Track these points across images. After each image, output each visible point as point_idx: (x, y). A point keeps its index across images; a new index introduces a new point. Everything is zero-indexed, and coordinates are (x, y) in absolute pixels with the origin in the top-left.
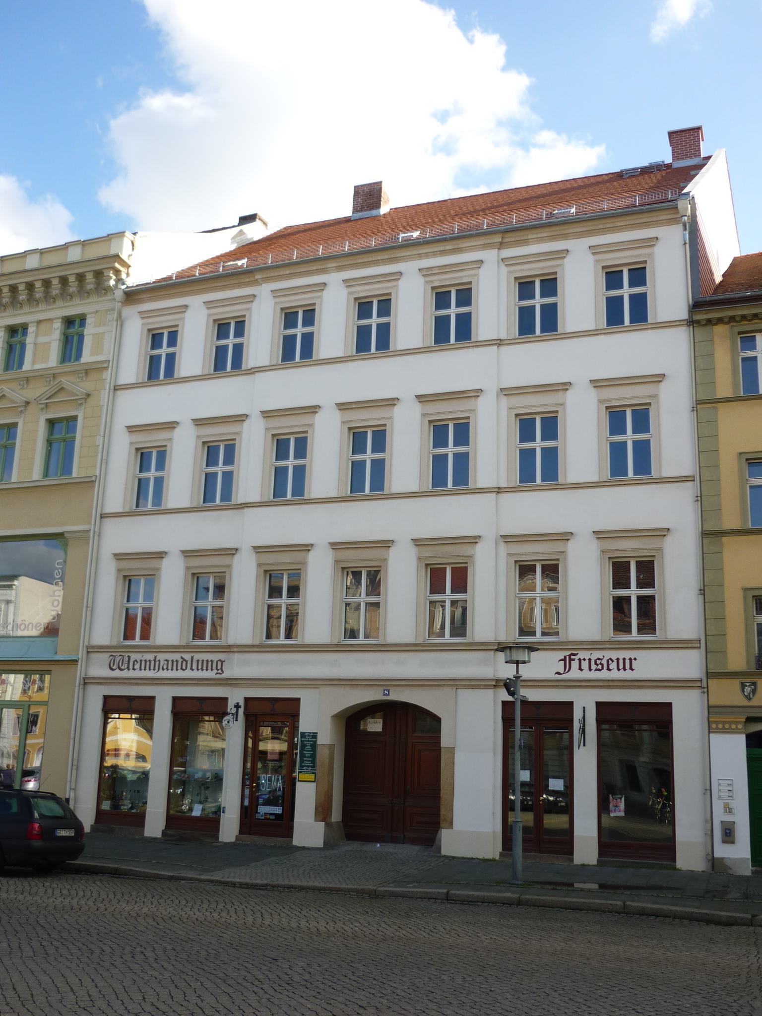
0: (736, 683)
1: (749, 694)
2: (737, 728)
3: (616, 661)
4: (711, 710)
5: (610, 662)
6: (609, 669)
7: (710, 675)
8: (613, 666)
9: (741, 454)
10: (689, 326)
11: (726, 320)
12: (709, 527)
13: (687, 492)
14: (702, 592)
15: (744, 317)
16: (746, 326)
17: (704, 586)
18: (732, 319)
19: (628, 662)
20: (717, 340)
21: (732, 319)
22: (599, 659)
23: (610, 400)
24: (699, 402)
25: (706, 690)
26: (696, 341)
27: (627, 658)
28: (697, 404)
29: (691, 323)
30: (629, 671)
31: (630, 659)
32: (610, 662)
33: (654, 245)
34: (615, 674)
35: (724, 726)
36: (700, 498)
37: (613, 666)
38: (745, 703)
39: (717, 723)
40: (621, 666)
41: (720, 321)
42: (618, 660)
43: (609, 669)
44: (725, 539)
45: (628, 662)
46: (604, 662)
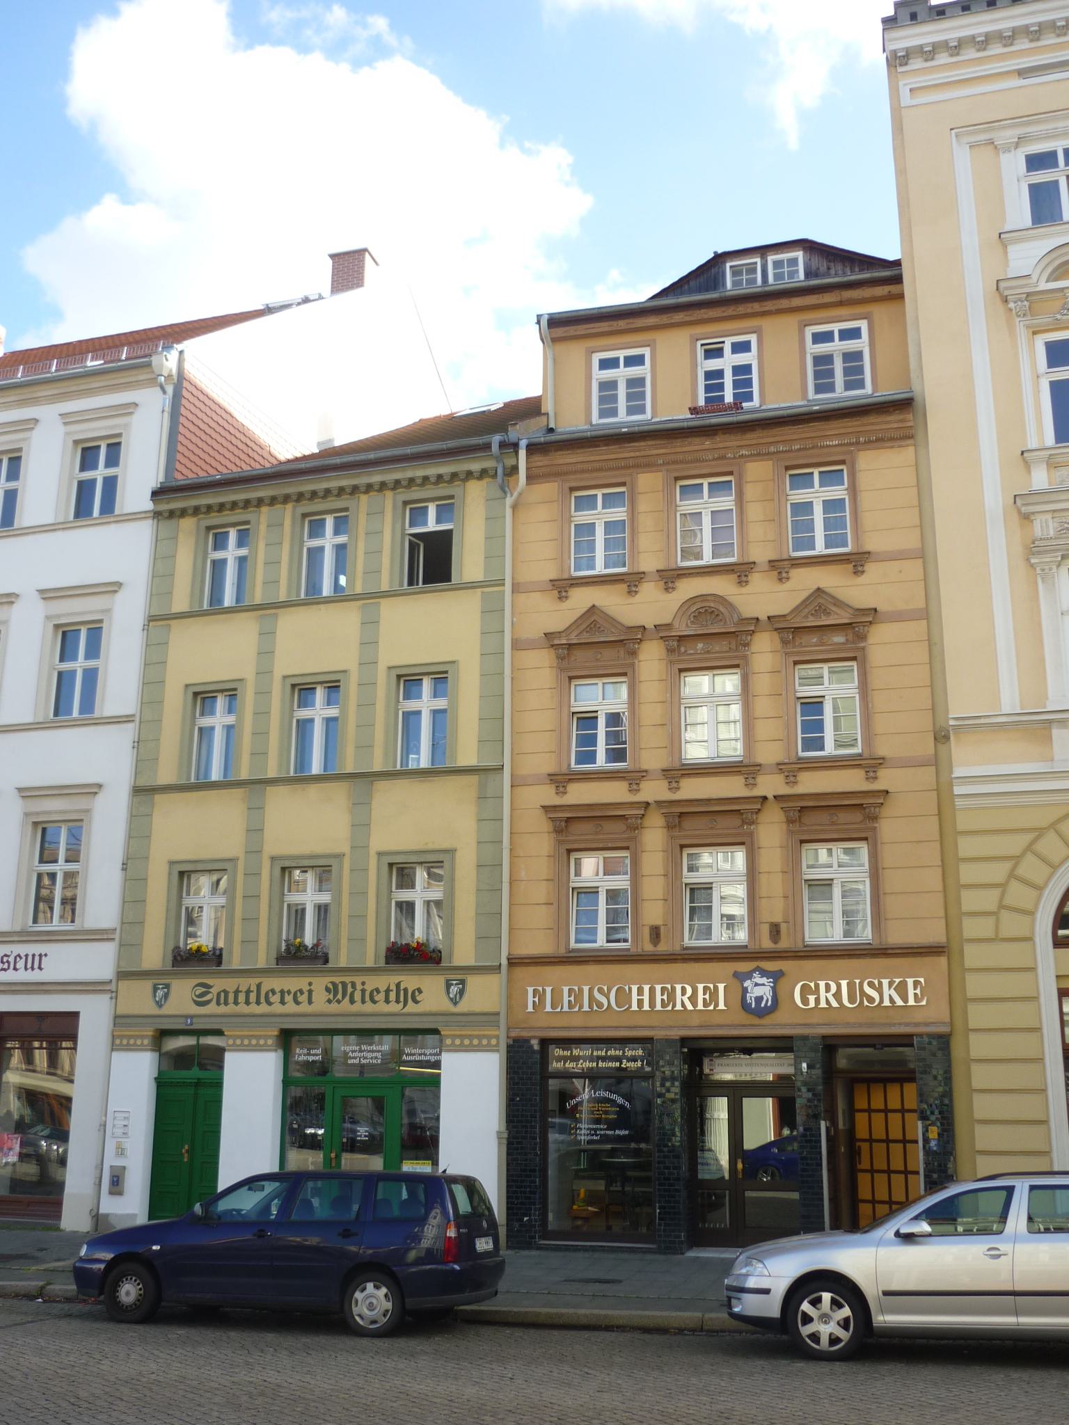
0: (147, 985)
1: (161, 999)
2: (142, 1043)
3: (24, 958)
4: (118, 1020)
5: (18, 959)
6: (15, 969)
7: (122, 975)
8: (20, 964)
9: (187, 686)
10: (154, 518)
11: (190, 511)
12: (143, 782)
13: (127, 733)
14: (125, 867)
15: (209, 508)
16: (215, 519)
17: (128, 859)
18: (196, 511)
19: (37, 959)
20: (181, 537)
21: (196, 511)
22: (6, 955)
23: (58, 616)
24: (152, 619)
25: (115, 995)
26: (159, 538)
27: (37, 954)
28: (149, 621)
29: (157, 515)
30: (37, 970)
31: (40, 956)
32: (18, 959)
33: (131, 413)
34: (22, 976)
35: (234, 1042)
36: (138, 743)
37: (20, 964)
38: (154, 1010)
39: (122, 1037)
40: (29, 965)
41: (183, 513)
42: (27, 956)
43: (15, 969)
44: (158, 798)
45: (37, 959)
46: (11, 959)
